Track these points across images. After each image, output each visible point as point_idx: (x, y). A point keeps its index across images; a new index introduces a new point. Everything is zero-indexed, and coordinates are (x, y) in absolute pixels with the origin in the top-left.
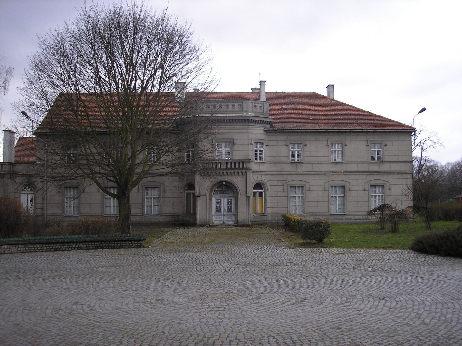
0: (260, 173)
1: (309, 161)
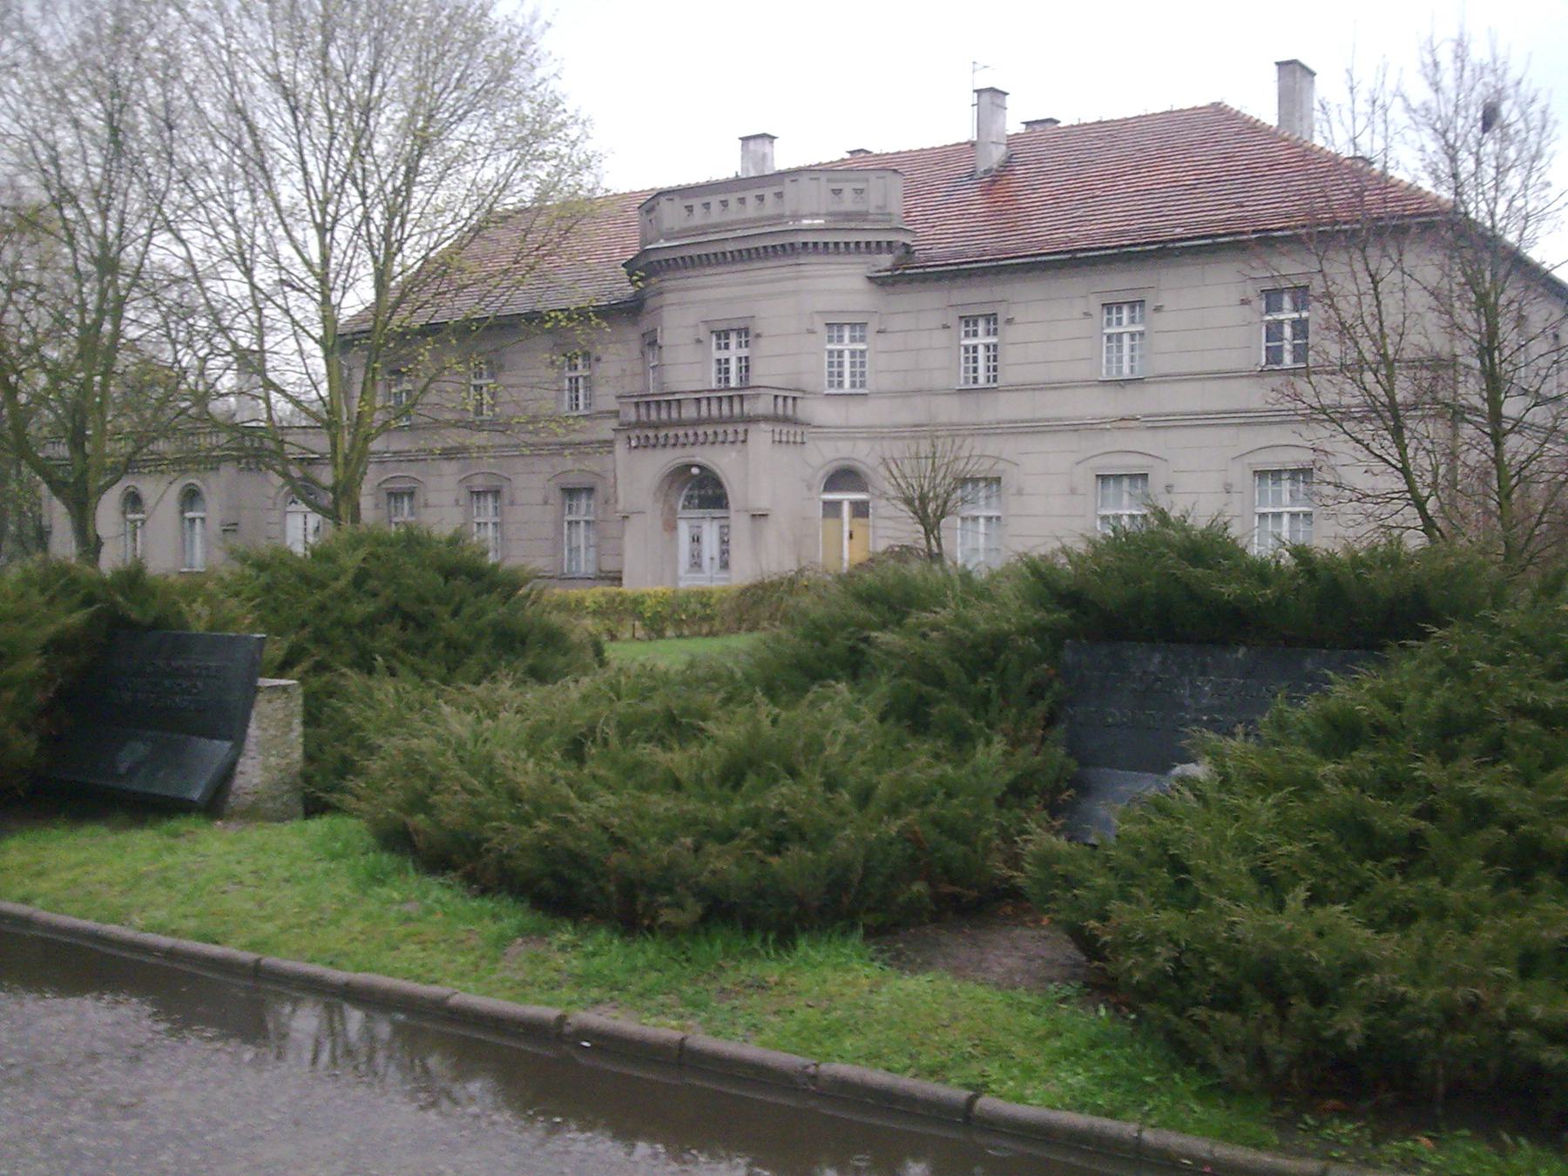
0: (847, 433)
1: (1021, 380)
